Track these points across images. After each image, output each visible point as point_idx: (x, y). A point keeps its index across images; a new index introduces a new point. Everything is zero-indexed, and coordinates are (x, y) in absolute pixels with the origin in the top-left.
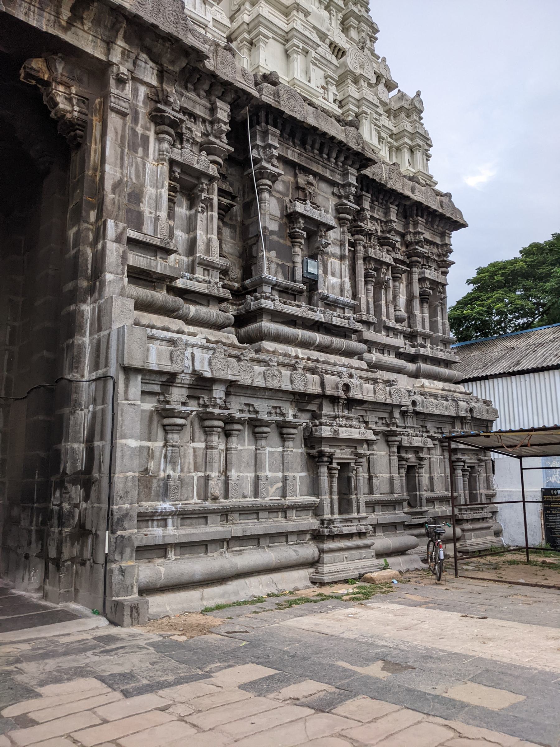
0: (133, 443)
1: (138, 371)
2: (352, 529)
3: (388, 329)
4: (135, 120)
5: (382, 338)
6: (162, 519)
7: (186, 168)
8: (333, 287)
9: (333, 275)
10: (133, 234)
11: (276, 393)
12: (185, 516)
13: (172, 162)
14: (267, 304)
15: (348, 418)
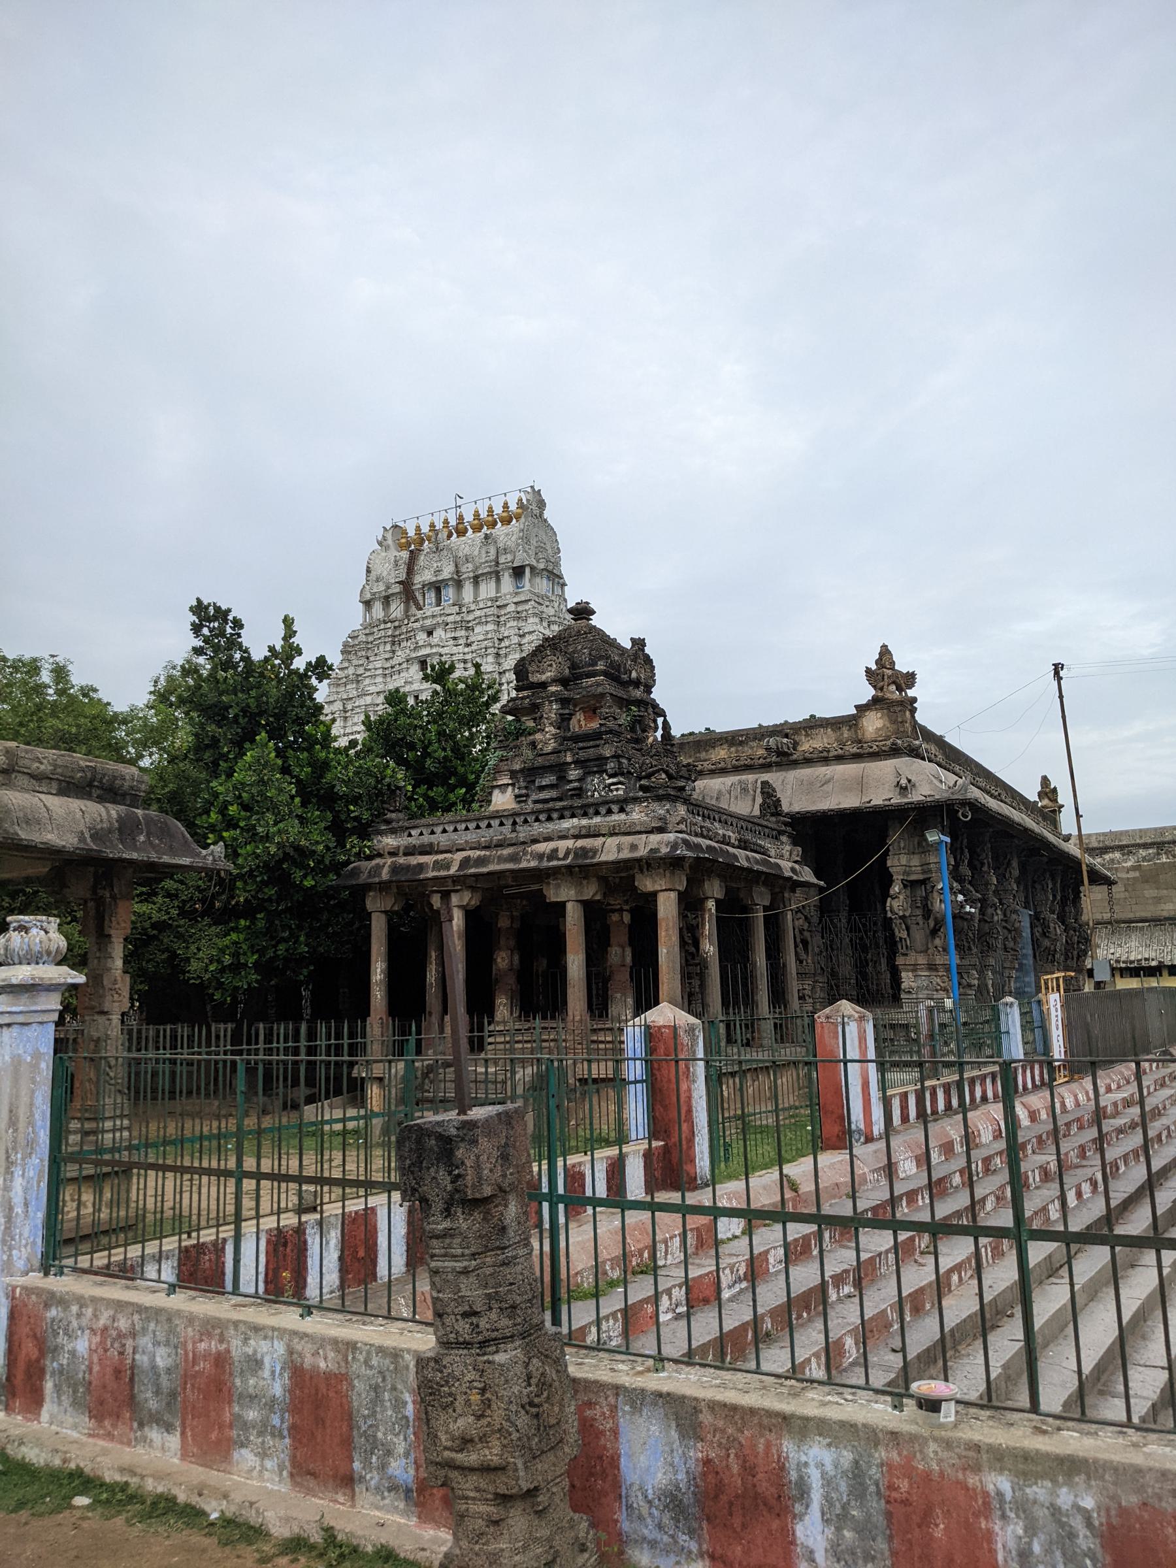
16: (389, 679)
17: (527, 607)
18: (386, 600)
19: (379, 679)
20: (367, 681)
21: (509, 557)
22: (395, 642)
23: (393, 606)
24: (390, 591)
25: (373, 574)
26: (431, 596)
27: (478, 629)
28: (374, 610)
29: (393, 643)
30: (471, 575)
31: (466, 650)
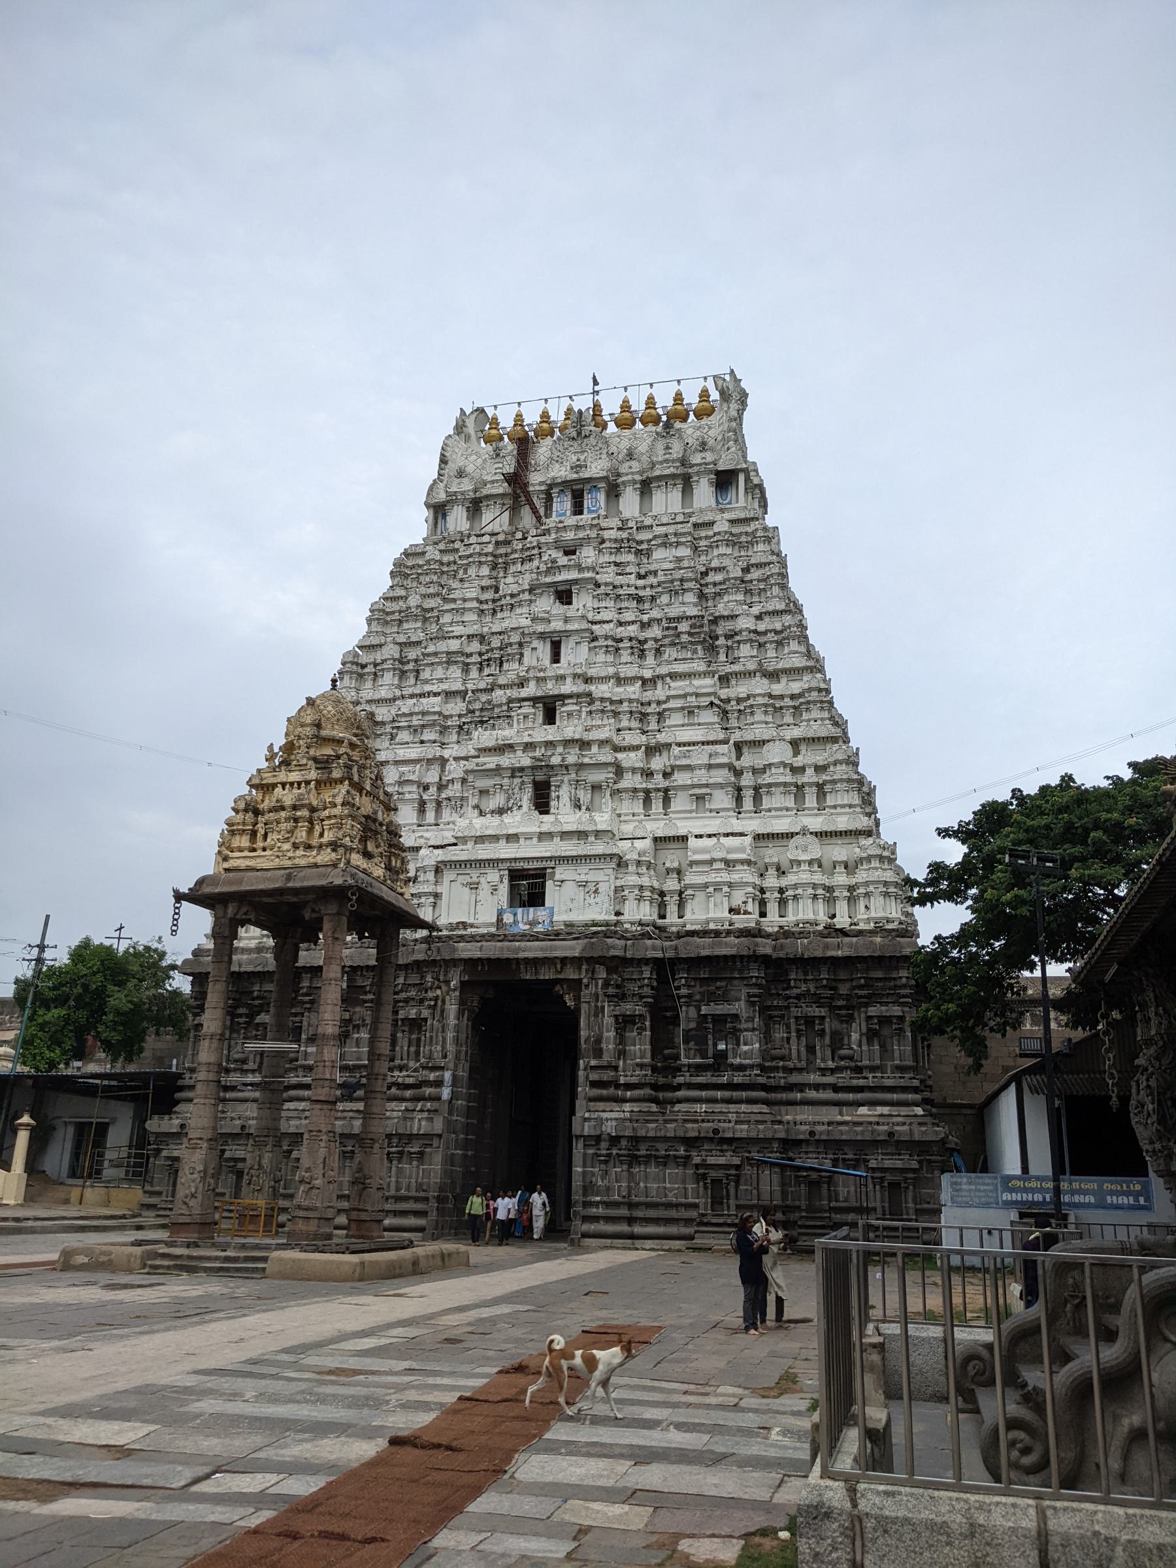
0: (580, 1169)
1: (581, 1136)
2: (721, 1221)
3: (820, 1069)
4: (597, 1000)
5: (814, 1078)
6: (597, 1204)
7: (624, 1016)
8: (745, 1052)
9: (745, 1044)
10: (593, 1063)
11: (665, 1139)
12: (608, 1205)
13: (616, 1016)
14: (680, 1080)
15: (722, 1151)
16: (488, 619)
17: (749, 530)
18: (475, 506)
19: (471, 617)
20: (447, 618)
21: (710, 457)
22: (499, 564)
23: (487, 516)
24: (485, 492)
25: (451, 468)
26: (563, 504)
27: (658, 554)
28: (450, 519)
29: (494, 567)
30: (638, 478)
31: (641, 583)
